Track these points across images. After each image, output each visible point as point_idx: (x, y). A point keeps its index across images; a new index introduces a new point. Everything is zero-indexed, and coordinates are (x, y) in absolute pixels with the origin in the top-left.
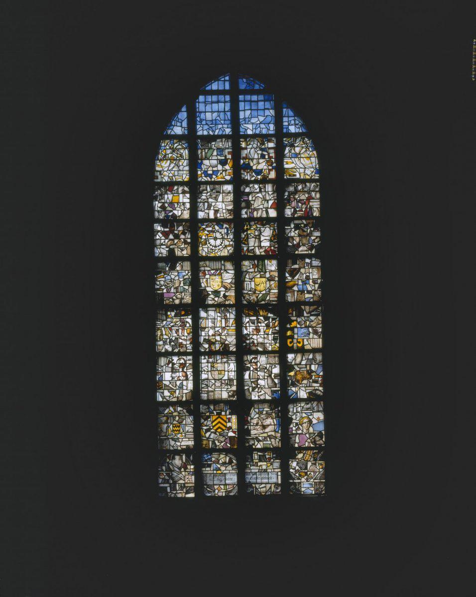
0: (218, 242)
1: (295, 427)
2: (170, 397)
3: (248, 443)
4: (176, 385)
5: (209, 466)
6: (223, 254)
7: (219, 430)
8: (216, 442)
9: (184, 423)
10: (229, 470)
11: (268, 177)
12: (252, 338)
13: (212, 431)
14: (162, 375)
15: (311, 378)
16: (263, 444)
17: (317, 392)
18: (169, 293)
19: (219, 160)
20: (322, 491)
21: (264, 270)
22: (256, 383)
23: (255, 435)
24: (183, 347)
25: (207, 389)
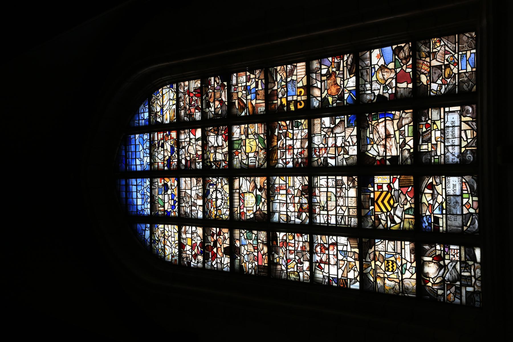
0: (219, 196)
1: (388, 90)
2: (354, 270)
3: (407, 159)
4: (342, 260)
5: (437, 219)
6: (228, 191)
7: (392, 202)
8: (406, 207)
9: (383, 253)
10: (442, 189)
11: (175, 139)
12: (296, 155)
13: (392, 212)
14: (332, 278)
15: (335, 72)
16: (408, 136)
17: (349, 63)
18: (258, 257)
19: (164, 192)
20: (472, 37)
21: (240, 141)
22: (340, 149)
23: (397, 149)
24: (305, 246)
25: (347, 217)
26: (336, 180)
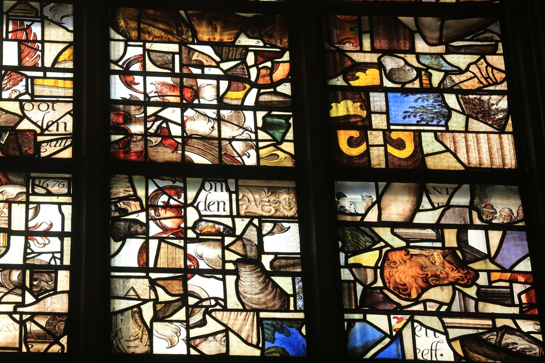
26: (56, 269)
